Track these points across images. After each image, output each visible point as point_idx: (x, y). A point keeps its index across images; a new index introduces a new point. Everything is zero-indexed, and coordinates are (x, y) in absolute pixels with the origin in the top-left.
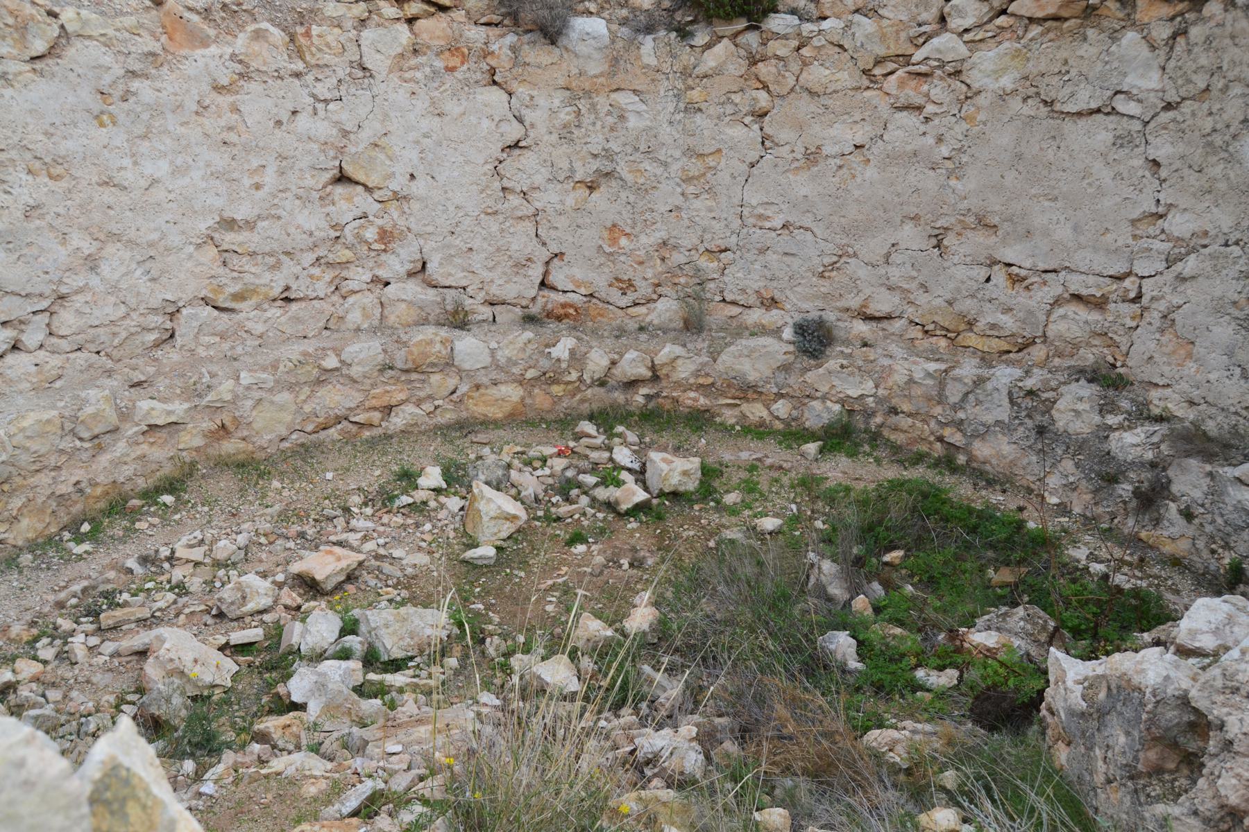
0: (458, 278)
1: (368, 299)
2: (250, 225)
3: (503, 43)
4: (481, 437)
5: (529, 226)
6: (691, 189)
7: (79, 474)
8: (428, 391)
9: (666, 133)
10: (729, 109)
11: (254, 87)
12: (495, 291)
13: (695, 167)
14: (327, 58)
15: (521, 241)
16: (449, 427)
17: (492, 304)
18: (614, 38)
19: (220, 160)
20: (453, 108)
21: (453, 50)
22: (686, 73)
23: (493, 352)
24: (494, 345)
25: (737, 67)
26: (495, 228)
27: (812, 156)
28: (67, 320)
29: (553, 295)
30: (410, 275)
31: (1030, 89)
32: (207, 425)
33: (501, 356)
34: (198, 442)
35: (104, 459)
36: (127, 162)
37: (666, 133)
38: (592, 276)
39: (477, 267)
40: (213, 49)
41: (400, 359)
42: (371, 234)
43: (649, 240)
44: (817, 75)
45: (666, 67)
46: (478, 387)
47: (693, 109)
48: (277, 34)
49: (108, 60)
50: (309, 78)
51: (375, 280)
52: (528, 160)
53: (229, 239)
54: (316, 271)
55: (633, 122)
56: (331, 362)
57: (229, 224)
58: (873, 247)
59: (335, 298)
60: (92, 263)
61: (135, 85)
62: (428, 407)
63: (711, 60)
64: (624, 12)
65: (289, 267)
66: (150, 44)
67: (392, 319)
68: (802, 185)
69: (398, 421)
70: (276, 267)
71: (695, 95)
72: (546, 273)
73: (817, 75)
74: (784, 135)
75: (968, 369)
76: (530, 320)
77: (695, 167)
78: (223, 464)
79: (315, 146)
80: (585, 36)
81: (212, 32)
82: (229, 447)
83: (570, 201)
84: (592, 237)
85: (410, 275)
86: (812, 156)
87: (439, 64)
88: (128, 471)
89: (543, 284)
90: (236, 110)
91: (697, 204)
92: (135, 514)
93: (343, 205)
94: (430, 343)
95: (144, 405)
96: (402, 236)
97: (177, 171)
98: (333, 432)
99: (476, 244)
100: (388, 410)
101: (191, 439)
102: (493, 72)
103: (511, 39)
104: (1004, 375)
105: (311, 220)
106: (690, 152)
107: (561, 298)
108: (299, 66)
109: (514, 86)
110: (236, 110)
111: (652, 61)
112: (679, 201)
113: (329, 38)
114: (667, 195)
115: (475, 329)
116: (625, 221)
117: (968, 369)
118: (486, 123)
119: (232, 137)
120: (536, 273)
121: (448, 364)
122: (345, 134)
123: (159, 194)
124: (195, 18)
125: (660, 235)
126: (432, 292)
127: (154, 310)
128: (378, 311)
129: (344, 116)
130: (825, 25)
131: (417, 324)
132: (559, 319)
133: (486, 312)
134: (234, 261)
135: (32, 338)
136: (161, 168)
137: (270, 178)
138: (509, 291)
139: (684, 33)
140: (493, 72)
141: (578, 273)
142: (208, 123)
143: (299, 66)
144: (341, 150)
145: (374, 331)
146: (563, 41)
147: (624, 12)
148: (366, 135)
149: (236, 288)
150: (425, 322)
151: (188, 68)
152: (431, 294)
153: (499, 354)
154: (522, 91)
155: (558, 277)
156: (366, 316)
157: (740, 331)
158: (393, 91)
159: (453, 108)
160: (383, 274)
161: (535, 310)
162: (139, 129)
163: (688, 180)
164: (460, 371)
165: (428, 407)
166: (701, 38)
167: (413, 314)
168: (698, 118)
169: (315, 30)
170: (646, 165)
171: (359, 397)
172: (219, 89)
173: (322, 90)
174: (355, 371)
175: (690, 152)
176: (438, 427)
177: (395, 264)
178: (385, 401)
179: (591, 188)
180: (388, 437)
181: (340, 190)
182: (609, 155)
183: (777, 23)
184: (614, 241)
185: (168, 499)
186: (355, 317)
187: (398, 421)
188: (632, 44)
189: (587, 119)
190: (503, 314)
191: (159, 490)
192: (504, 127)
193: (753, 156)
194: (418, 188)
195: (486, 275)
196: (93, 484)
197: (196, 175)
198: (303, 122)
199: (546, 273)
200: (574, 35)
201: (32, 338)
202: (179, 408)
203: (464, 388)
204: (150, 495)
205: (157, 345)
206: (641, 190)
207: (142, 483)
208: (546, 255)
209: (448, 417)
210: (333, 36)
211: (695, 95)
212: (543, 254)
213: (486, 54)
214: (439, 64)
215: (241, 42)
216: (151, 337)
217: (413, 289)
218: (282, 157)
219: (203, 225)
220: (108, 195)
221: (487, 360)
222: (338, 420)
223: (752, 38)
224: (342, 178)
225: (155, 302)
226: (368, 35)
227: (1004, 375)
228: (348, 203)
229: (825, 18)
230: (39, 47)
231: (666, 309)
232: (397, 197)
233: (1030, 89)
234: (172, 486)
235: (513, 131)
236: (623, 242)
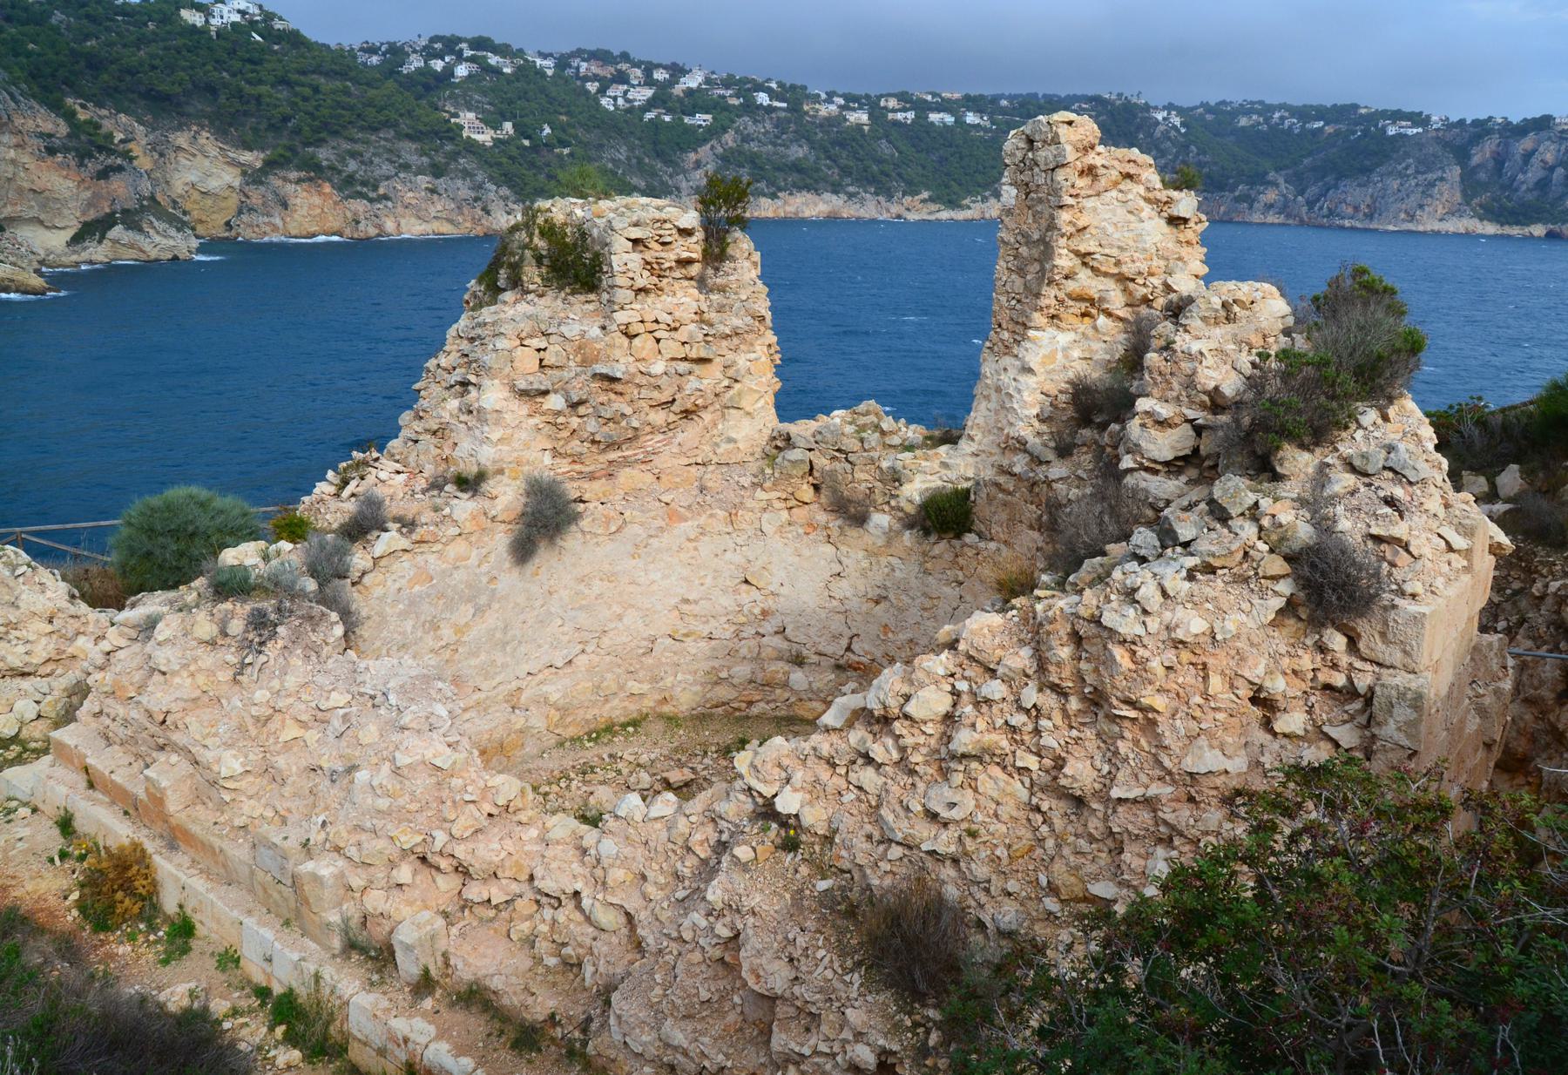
0: (801, 638)
1: (753, 643)
2: (696, 602)
3: (835, 523)
4: (796, 728)
5: (842, 617)
6: (926, 614)
7: (596, 711)
8: (773, 697)
9: (914, 583)
10: (945, 577)
11: (706, 539)
12: (820, 648)
13: (928, 604)
14: (744, 526)
16: (782, 718)
17: (820, 655)
18: (891, 529)
19: (685, 572)
20: (807, 553)
21: (810, 525)
22: (924, 554)
23: (810, 683)
24: (811, 679)
25: (949, 556)
26: (824, 616)
28: (606, 641)
29: (852, 656)
30: (776, 633)
32: (659, 697)
33: (815, 686)
34: (652, 704)
35: (608, 706)
36: (643, 574)
37: (914, 583)
38: (873, 650)
39: (811, 634)
40: (690, 523)
41: (760, 677)
42: (757, 611)
43: (903, 637)
45: (915, 549)
46: (801, 700)
47: (927, 572)
48: (721, 514)
49: (640, 532)
50: (734, 535)
51: (757, 633)
52: (844, 583)
53: (685, 608)
54: (726, 626)
55: (898, 574)
56: (724, 675)
57: (686, 601)
59: (736, 640)
60: (620, 617)
61: (652, 540)
62: (772, 705)
63: (937, 550)
64: (901, 514)
65: (713, 623)
66: (659, 523)
67: (763, 655)
69: (755, 710)
70: (707, 622)
71: (929, 565)
72: (850, 644)
74: (968, 598)
76: (838, 667)
77: (928, 604)
78: (661, 716)
79: (733, 567)
80: (877, 526)
81: (690, 515)
82: (666, 709)
83: (864, 608)
84: (874, 629)
85: (776, 633)
87: (801, 531)
88: (618, 712)
89: (849, 649)
90: (696, 549)
91: (928, 623)
92: (615, 734)
93: (744, 595)
94: (778, 672)
95: (630, 683)
96: (773, 613)
97: (665, 577)
98: (720, 710)
99: (812, 623)
100: (750, 703)
101: (648, 703)
102: (829, 536)
103: (839, 522)
105: (727, 602)
106: (925, 595)
107: (856, 659)
108: (730, 529)
109: (839, 545)
110: (696, 549)
111: (909, 544)
112: (920, 619)
113: (747, 518)
115: (806, 668)
116: (892, 623)
118: (823, 562)
119: (693, 562)
120: (844, 642)
121: (785, 685)
122: (749, 561)
123: (655, 587)
124: (682, 510)
125: (909, 635)
126: (786, 643)
127: (644, 639)
128: (756, 650)
129: (749, 554)
130: (992, 545)
131: (777, 659)
132: (855, 669)
133: (815, 658)
134: (686, 618)
135: (589, 649)
136: (656, 576)
137: (708, 581)
138: (829, 650)
140: (829, 536)
141: (867, 647)
142: (683, 556)
143: (730, 529)
144: (745, 569)
145: (753, 660)
146: (865, 526)
147: (901, 514)
148: (759, 563)
149: (685, 631)
150: (781, 659)
151: (676, 532)
152: (785, 645)
153: (814, 685)
154: (844, 549)
155: (855, 647)
156: (750, 652)
158: (776, 542)
159: (807, 553)
160: (761, 631)
161: (842, 662)
162: (650, 559)
163: (925, 609)
164: (792, 689)
165: (772, 705)
166: (933, 538)
167: (775, 654)
168: (930, 578)
169: (740, 512)
170: (903, 597)
171: (736, 694)
172: (689, 540)
173: (739, 541)
174: (735, 681)
175: (925, 595)
176: (776, 717)
177: (768, 627)
178: (749, 698)
179: (877, 602)
180: (748, 717)
181: (745, 587)
182: (885, 588)
183: (970, 538)
184: (886, 634)
185: (631, 729)
186: (744, 651)
187: (755, 710)
188: (899, 533)
189: (875, 568)
190: (825, 662)
191: (629, 724)
192: (833, 565)
193: (955, 604)
194: (783, 591)
195: (817, 640)
196: (602, 716)
197: (673, 579)
198: (729, 555)
199: (850, 644)
200: (871, 524)
201: (589, 649)
202: (646, 687)
203: (793, 699)
204: (624, 726)
205: (644, 654)
206: (899, 609)
207: (622, 719)
208: (850, 634)
209: (783, 713)
210: (748, 516)
211: (929, 565)
212: (848, 633)
213: (826, 528)
214: (801, 531)
215: (703, 520)
216: (641, 651)
217: (777, 641)
218: (715, 571)
219: (673, 601)
220: (631, 588)
221: (806, 687)
222: (724, 704)
223: (955, 542)
224: (746, 582)
225: (645, 635)
226: (766, 516)
228: (747, 596)
229: (992, 539)
230: (613, 529)
232: (772, 594)
234: (635, 723)
235: (837, 568)
236: (890, 635)
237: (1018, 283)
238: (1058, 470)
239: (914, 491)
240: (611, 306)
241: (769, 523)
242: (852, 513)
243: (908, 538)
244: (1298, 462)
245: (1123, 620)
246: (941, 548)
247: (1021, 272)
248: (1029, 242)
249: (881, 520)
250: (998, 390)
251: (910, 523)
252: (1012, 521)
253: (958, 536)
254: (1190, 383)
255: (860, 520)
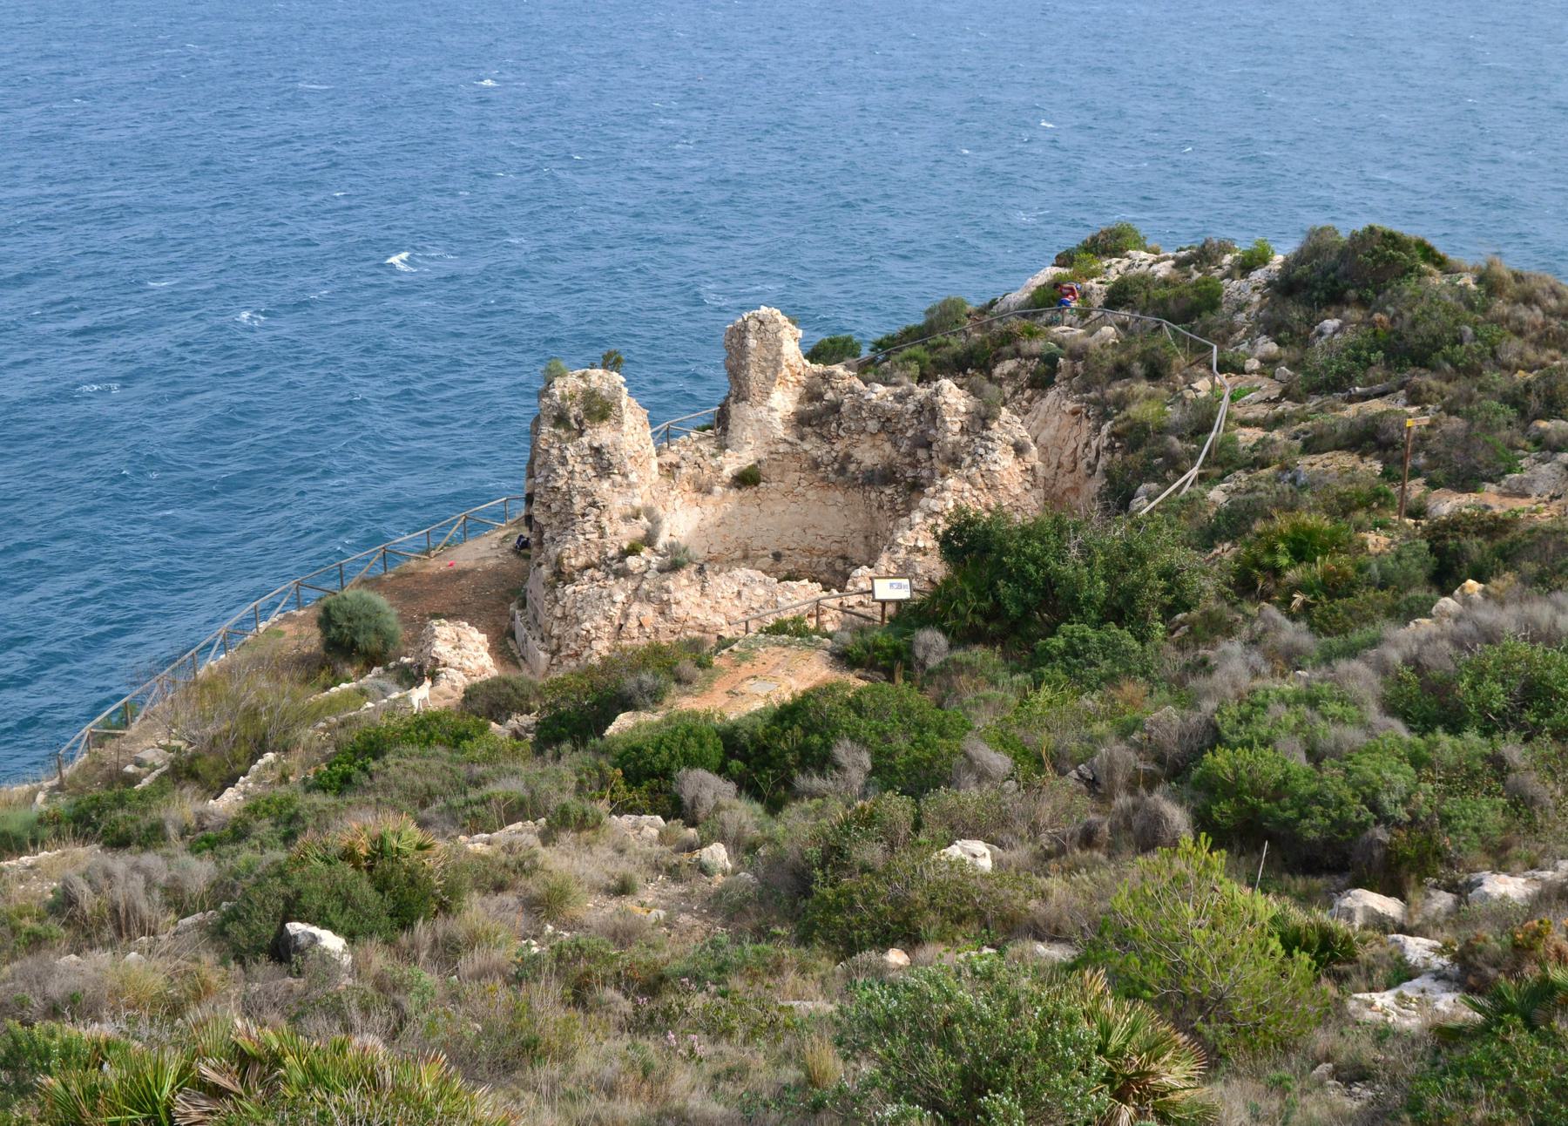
15: (704, 543)
27: (773, 514)
31: (820, 499)
44: (772, 496)
58: (789, 533)
68: (770, 520)
73: (772, 496)
75: (815, 559)
86: (773, 514)
104: (824, 560)
114: (737, 526)
117: (815, 559)
139: (739, 488)
157: (758, 557)
227: (824, 560)
231: (738, 554)
233: (820, 499)
237: (762, 377)
238: (807, 446)
239: (729, 471)
240: (620, 422)
241: (678, 502)
242: (704, 489)
243: (732, 492)
244: (995, 425)
245: (997, 468)
246: (748, 492)
247: (763, 372)
248: (766, 360)
249: (718, 489)
250: (758, 421)
251: (730, 486)
252: (783, 472)
253: (756, 484)
254: (957, 411)
255: (709, 492)
